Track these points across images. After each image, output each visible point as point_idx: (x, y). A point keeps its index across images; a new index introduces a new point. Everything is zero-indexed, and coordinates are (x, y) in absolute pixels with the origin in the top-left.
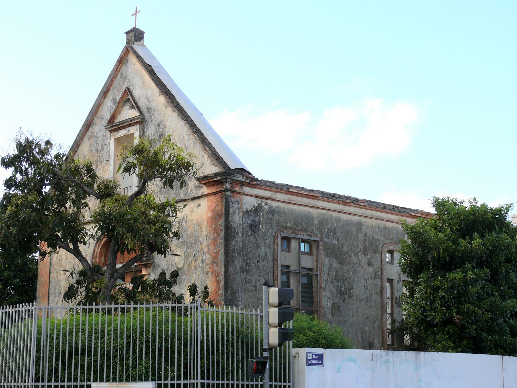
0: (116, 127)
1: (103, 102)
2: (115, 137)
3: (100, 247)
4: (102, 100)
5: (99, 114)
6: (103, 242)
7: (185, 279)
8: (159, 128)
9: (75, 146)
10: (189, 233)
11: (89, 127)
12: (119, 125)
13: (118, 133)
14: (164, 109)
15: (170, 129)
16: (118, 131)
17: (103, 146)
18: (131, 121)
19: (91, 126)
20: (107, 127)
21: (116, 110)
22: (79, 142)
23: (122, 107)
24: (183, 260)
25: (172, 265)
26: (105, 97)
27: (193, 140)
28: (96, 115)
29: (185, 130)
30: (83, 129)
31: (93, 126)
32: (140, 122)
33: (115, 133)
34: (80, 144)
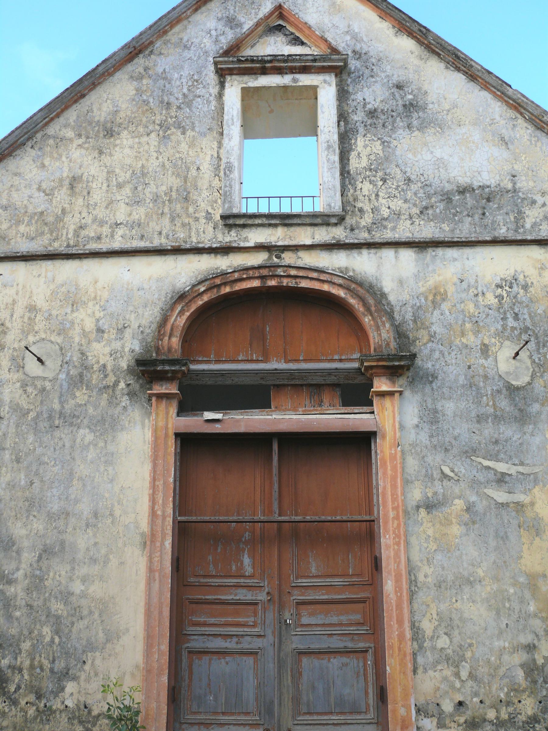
0: (258, 65)
1: (187, 17)
2: (245, 86)
3: (188, 314)
4: (189, 13)
5: (173, 35)
6: (200, 303)
7: (539, 413)
8: (401, 92)
9: (86, 83)
10: (539, 311)
11: (137, 55)
12: (270, 61)
13: (257, 79)
14: (416, 62)
15: (442, 100)
16: (253, 76)
17: (191, 97)
18: (315, 60)
19: (141, 56)
20: (221, 59)
21: (248, 35)
22: (100, 78)
23: (260, 37)
24: (527, 368)
25: (486, 377)
26: (196, 10)
27: (529, 131)
28: (162, 36)
29: (497, 109)
30: (122, 54)
31: (149, 55)
32: (338, 71)
33: (246, 78)
34: (99, 83)
